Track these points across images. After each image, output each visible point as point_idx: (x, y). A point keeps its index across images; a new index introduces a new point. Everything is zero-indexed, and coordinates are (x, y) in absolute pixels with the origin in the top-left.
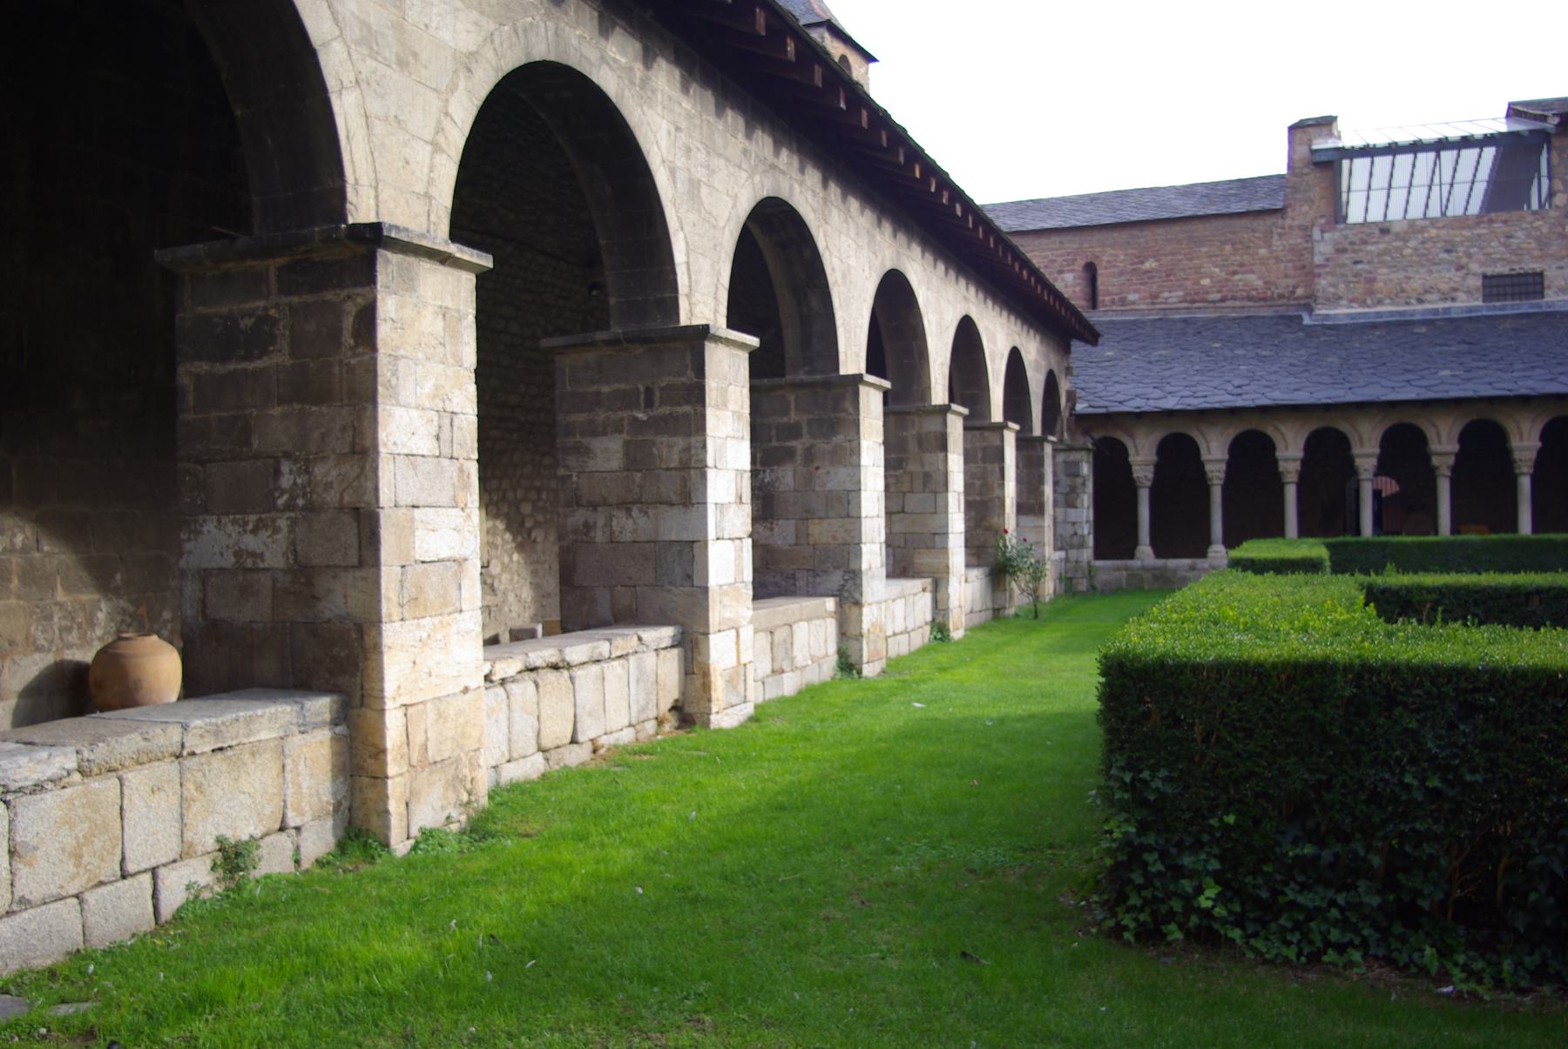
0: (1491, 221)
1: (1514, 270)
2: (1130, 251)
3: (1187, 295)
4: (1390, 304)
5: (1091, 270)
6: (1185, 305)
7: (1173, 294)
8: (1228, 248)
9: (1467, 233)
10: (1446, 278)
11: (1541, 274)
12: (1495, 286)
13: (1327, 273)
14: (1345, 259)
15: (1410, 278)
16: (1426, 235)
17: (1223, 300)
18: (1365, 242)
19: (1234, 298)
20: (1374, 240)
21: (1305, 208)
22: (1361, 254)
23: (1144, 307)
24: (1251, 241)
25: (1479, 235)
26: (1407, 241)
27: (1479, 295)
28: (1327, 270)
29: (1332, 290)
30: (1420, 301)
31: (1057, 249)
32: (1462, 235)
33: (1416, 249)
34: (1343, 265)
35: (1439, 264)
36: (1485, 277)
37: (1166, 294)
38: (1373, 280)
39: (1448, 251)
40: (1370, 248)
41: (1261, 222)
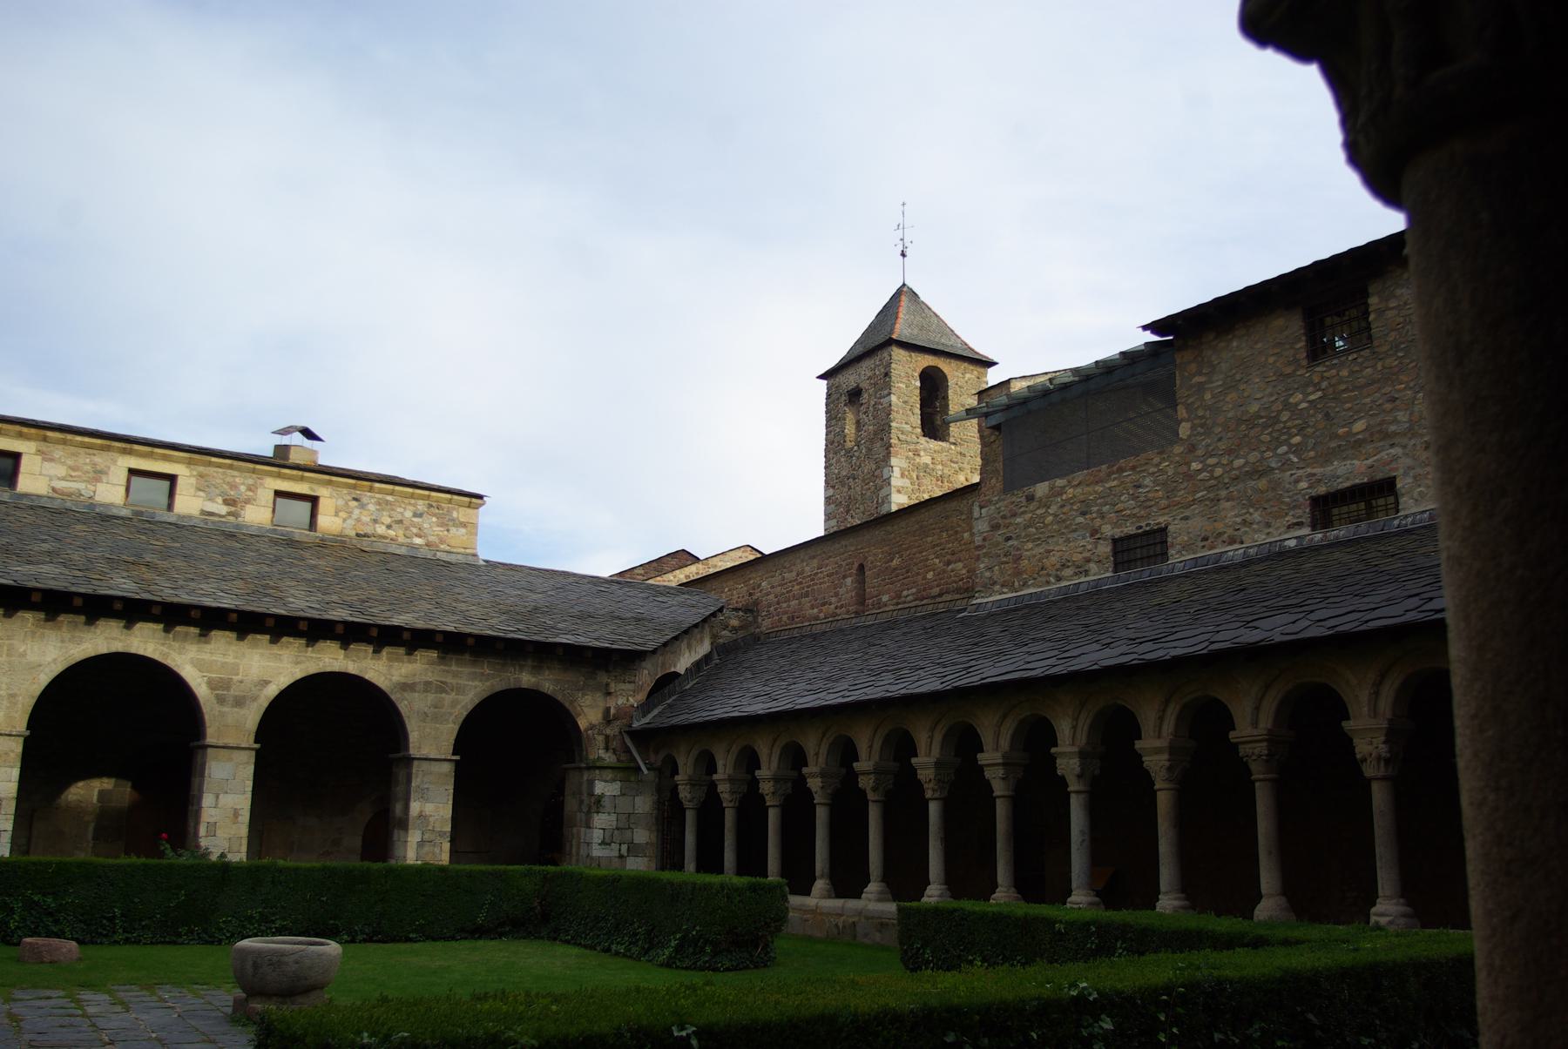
0: (1121, 470)
1: (1141, 527)
2: (886, 548)
3: (919, 591)
4: (1033, 585)
5: (861, 568)
6: (917, 602)
7: (910, 592)
8: (944, 534)
9: (1099, 488)
10: (1079, 547)
11: (1163, 530)
12: (1127, 551)
13: (986, 555)
14: (998, 536)
15: (1049, 551)
16: (1064, 497)
17: (940, 595)
18: (1014, 515)
19: (947, 592)
20: (1023, 509)
21: (994, 481)
22: (1011, 528)
23: (892, 608)
24: (960, 526)
25: (1110, 488)
26: (1049, 508)
27: (1110, 566)
28: (985, 551)
29: (988, 574)
30: (1059, 579)
31: (843, 554)
32: (1096, 492)
33: (1055, 515)
34: (998, 544)
35: (1075, 531)
36: (1115, 541)
37: (905, 593)
38: (1020, 558)
39: (1083, 514)
40: (1019, 520)
41: (965, 502)
